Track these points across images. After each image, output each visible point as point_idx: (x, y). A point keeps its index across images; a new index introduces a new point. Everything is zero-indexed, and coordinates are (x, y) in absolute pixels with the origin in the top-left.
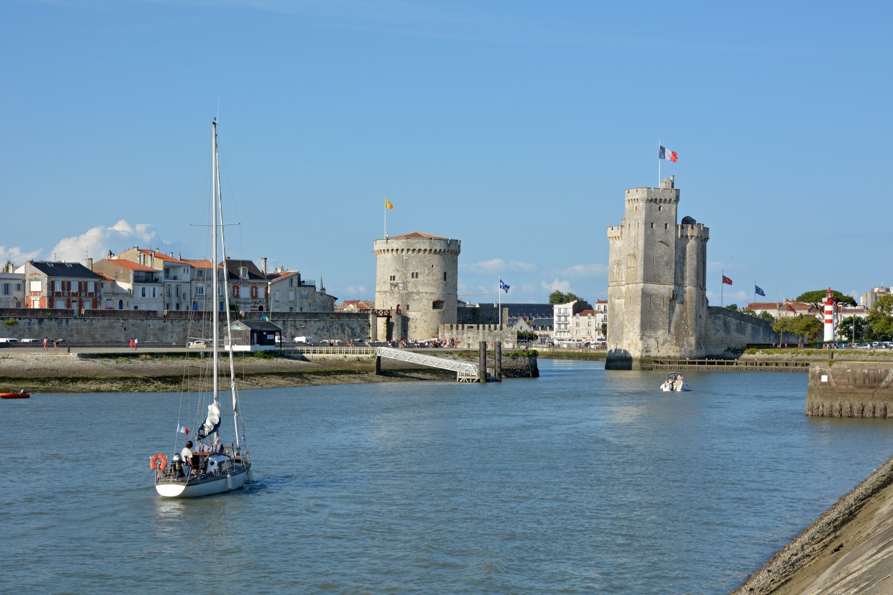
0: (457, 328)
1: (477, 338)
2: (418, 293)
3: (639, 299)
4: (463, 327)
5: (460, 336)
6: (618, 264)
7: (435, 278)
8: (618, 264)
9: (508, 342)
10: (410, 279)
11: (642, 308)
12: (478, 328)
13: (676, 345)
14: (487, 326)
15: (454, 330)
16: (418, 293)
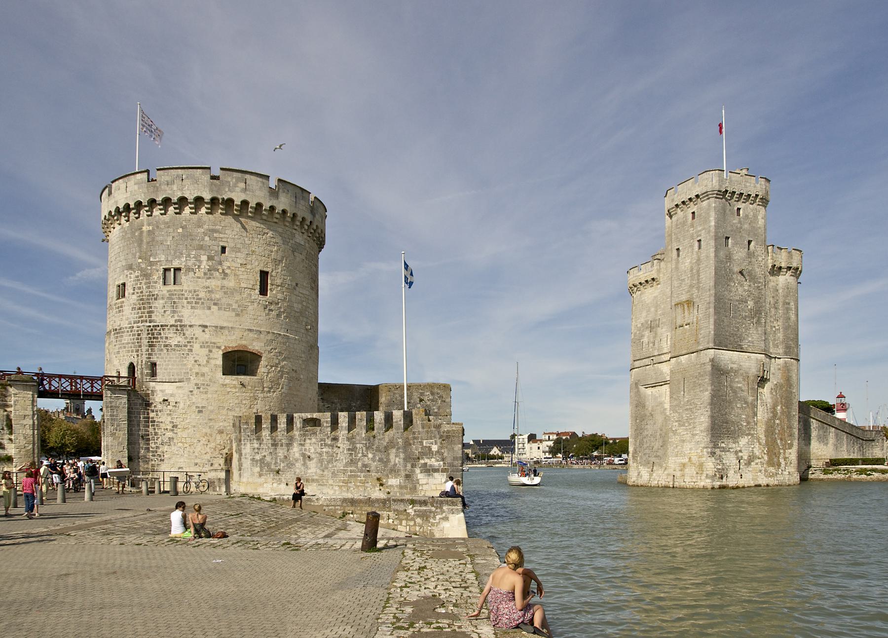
0: (274, 428)
1: (332, 458)
2: (179, 328)
3: (707, 379)
4: (290, 421)
5: (281, 452)
6: (652, 326)
7: (231, 283)
8: (652, 326)
9: (429, 471)
10: (160, 289)
11: (713, 396)
12: (335, 423)
13: (770, 463)
14: (361, 415)
15: (266, 433)
16: (179, 328)
